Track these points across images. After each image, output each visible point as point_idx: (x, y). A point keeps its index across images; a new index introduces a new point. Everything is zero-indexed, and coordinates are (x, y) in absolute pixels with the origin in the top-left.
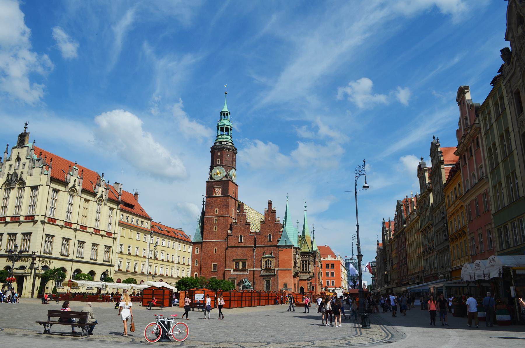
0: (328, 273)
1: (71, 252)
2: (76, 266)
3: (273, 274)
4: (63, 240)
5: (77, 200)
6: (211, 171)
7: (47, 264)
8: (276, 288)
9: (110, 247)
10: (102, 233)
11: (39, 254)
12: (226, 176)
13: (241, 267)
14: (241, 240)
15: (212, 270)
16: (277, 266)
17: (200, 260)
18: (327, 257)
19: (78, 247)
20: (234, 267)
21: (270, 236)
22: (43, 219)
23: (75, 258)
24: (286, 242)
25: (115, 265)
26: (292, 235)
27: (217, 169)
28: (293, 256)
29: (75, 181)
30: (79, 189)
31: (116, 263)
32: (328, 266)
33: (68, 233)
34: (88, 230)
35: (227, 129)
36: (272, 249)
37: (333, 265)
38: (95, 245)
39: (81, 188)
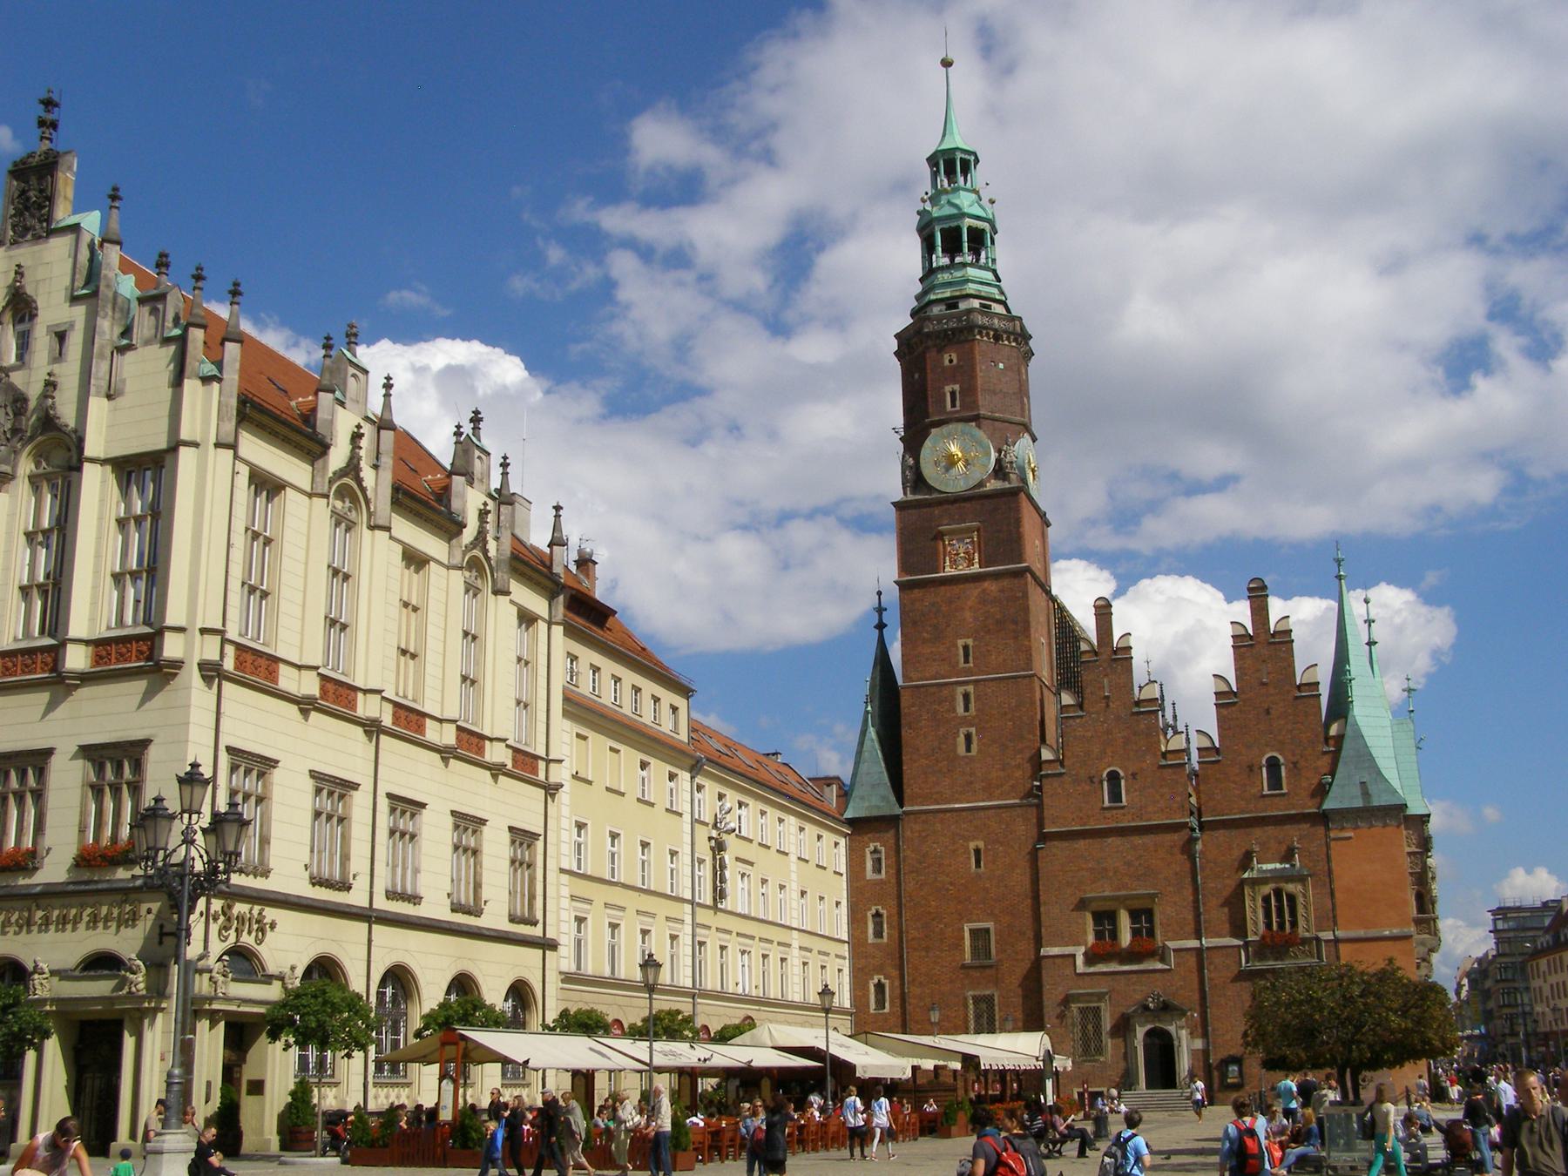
1: (359, 864)
4: (318, 791)
5: (377, 555)
7: (248, 940)
10: (496, 754)
12: (1000, 471)
13: (1126, 938)
14: (1115, 796)
19: (392, 833)
20: (1091, 939)
21: (1273, 765)
22: (209, 649)
23: (381, 903)
24: (1366, 794)
25: (563, 940)
27: (950, 437)
29: (356, 437)
31: (564, 927)
33: (343, 749)
34: (433, 733)
36: (1294, 834)
38: (467, 823)
39: (387, 477)
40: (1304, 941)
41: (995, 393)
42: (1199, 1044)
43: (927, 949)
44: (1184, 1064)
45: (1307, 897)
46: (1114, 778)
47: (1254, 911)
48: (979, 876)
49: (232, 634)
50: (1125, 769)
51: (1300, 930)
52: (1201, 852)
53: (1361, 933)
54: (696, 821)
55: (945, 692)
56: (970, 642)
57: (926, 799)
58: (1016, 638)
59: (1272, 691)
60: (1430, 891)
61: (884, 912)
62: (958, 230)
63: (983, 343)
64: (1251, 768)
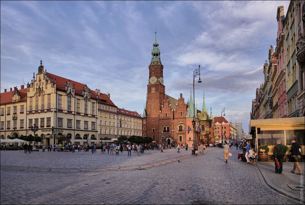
1: (73, 125)
2: (77, 132)
6: (150, 79)
9: (94, 122)
10: (89, 115)
11: (55, 127)
13: (166, 130)
14: (166, 116)
17: (146, 128)
21: (181, 112)
22: (55, 110)
23: (76, 129)
24: (190, 116)
29: (70, 90)
30: (73, 94)
33: (71, 117)
34: (81, 114)
38: (86, 122)
39: (74, 93)
44: (171, 143)
46: (166, 114)
49: (57, 108)
54: (118, 119)
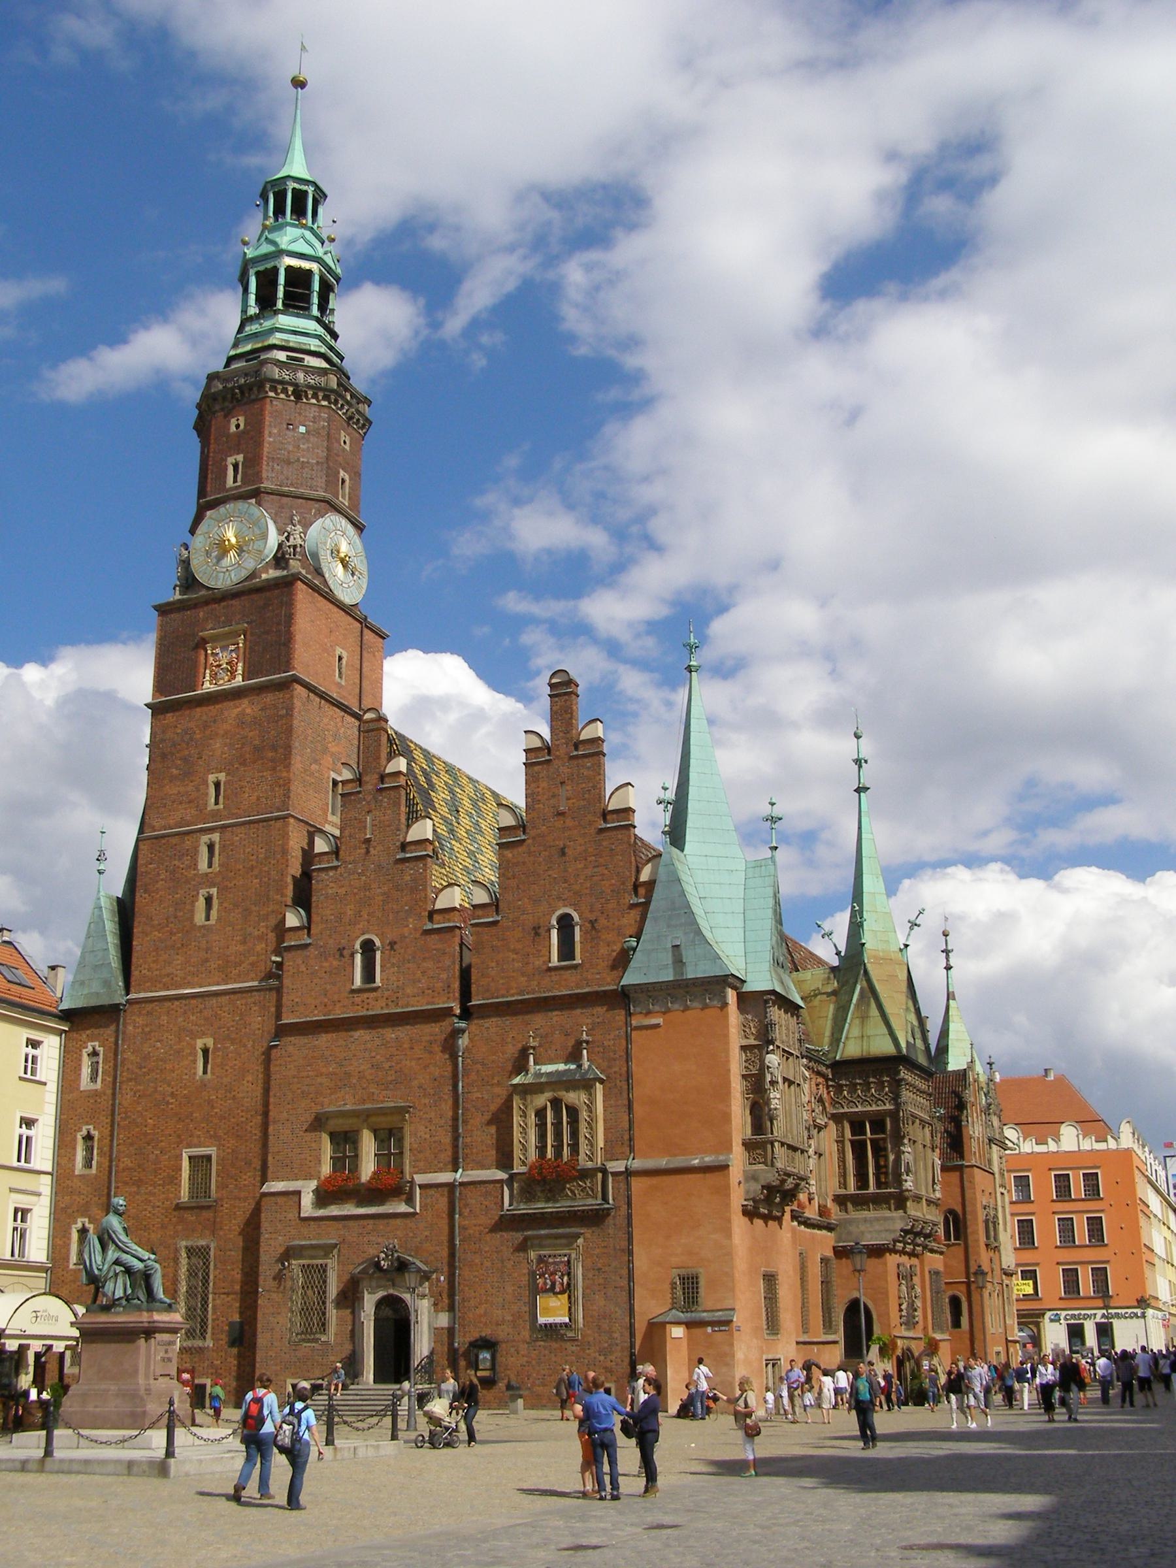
0: (1067, 1227)
3: (594, 1202)
8: (621, 1313)
13: (368, 1168)
15: (184, 1194)
16: (624, 1140)
18: (1057, 1139)
20: (326, 1169)
21: (566, 924)
24: (679, 962)
26: (726, 911)
27: (227, 519)
28: (736, 1065)
32: (1063, 1183)
35: (299, 278)
37: (1091, 1180)
40: (585, 1174)
41: (289, 463)
42: (443, 1320)
43: (139, 1183)
45: (598, 1105)
46: (368, 948)
47: (524, 1132)
48: (204, 1085)
50: (381, 936)
51: (582, 1157)
52: (467, 1049)
53: (663, 1162)
55: (188, 842)
56: (222, 777)
57: (155, 983)
58: (274, 769)
59: (569, 822)
60: (768, 1102)
61: (96, 1134)
62: (275, 270)
63: (277, 404)
64: (538, 932)
